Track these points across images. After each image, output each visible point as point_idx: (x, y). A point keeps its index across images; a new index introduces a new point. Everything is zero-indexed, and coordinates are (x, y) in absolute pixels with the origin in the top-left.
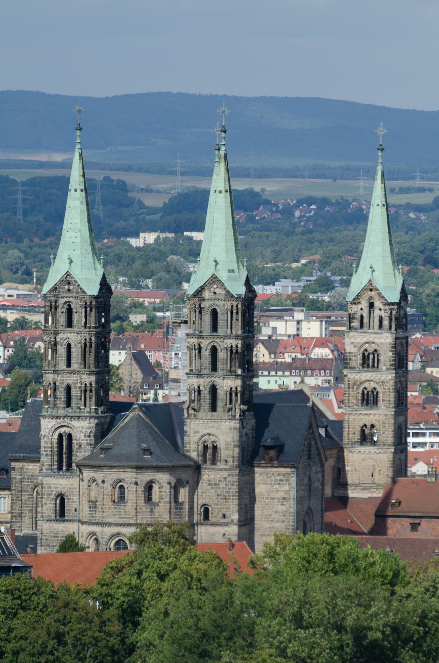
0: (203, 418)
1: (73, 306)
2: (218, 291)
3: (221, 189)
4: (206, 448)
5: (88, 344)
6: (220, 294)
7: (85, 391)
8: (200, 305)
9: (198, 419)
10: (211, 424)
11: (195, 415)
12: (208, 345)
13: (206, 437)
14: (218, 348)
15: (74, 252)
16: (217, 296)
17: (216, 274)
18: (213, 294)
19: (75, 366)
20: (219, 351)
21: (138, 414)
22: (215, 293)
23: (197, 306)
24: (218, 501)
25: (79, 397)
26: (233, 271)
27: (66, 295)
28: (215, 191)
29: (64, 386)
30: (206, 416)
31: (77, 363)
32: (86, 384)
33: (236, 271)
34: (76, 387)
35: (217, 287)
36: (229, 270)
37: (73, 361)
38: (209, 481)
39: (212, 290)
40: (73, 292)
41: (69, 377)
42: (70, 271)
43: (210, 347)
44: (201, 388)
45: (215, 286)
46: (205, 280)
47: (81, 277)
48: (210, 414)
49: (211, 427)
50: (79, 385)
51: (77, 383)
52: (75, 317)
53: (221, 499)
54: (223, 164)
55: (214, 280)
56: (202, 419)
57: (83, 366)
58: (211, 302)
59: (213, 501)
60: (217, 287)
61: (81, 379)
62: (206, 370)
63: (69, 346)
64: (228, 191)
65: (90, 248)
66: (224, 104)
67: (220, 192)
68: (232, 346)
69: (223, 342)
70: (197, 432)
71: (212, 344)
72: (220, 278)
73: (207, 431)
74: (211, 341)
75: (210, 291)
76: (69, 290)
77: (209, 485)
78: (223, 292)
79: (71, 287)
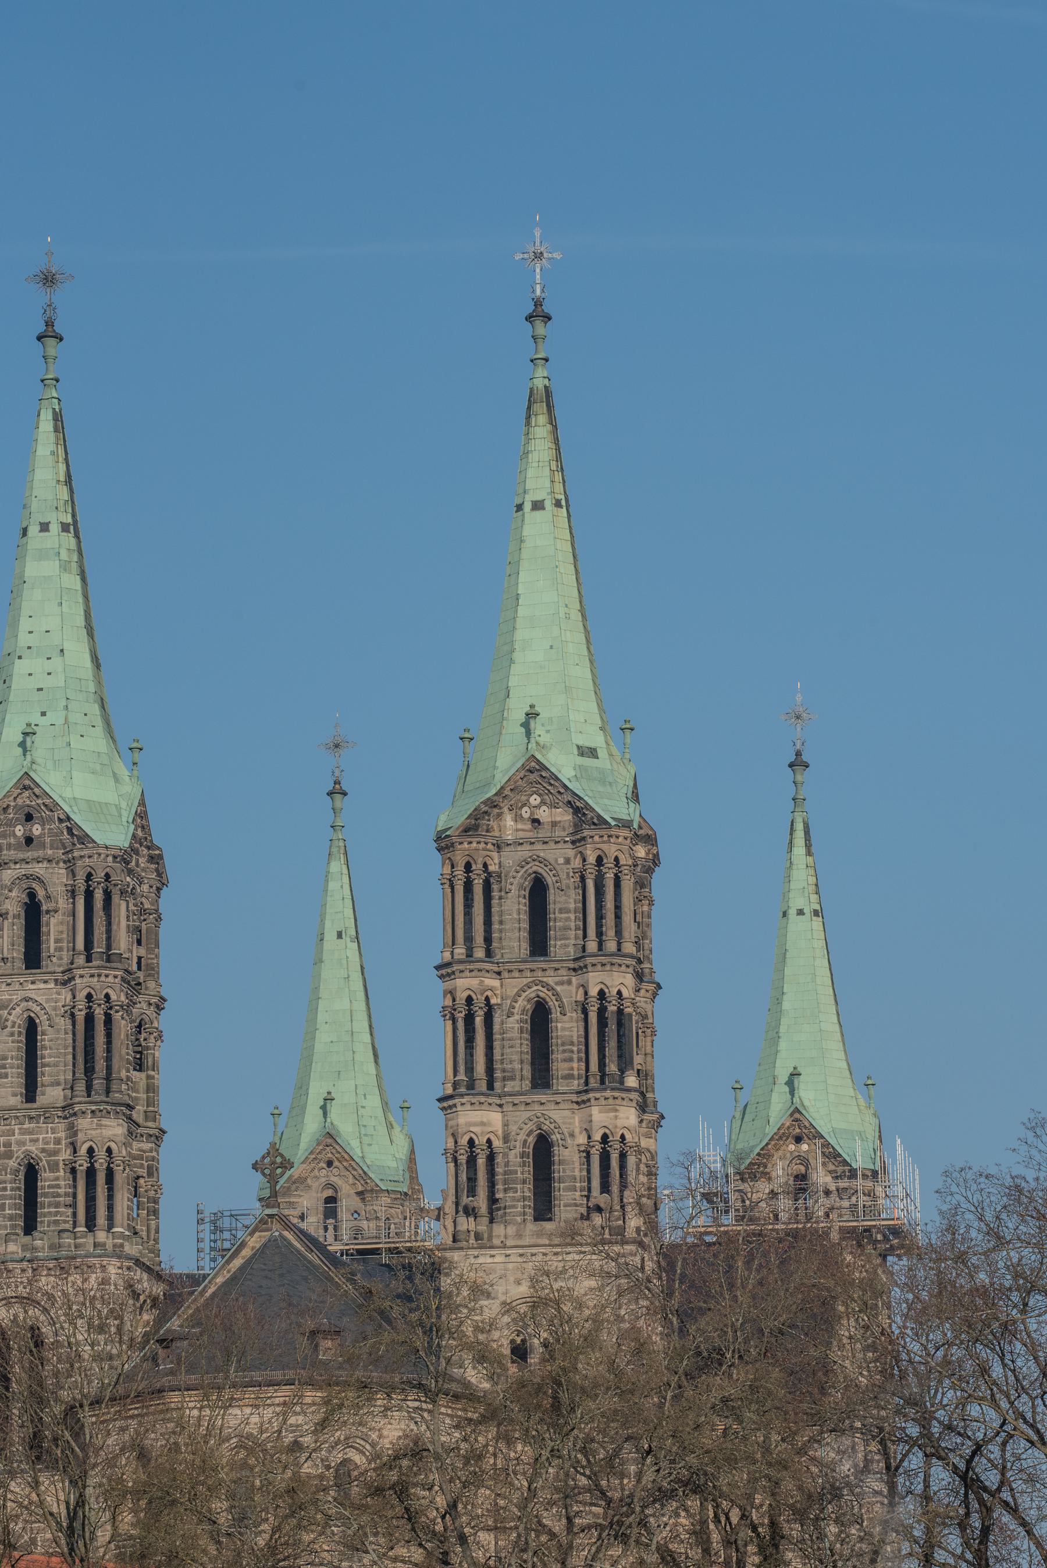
0: (509, 1243)
1: (41, 894)
2: (544, 814)
3: (538, 497)
5: (99, 1012)
6: (554, 824)
7: (91, 1173)
8: (485, 865)
9: (492, 1247)
11: (478, 1237)
14: (552, 1004)
15: (42, 721)
16: (543, 833)
17: (539, 757)
18: (529, 826)
19: (51, 1095)
20: (555, 1014)
21: (281, 1235)
22: (536, 822)
23: (477, 867)
25: (69, 1200)
26: (592, 753)
27: (21, 855)
28: (519, 508)
29: (12, 1163)
30: (519, 1236)
31: (58, 1084)
32: (91, 1151)
33: (602, 753)
34: (54, 1167)
35: (543, 803)
36: (578, 747)
37: (45, 1076)
39: (526, 812)
40: (43, 846)
41: (31, 1133)
42: (32, 774)
43: (521, 1003)
44: (497, 1143)
46: (500, 779)
47: (68, 793)
48: (531, 1227)
50: (65, 1155)
51: (56, 1153)
52: (54, 927)
54: (542, 419)
55: (533, 777)
56: (504, 1246)
57: (81, 1086)
58: (524, 852)
60: (543, 803)
61: (75, 1134)
62: (512, 1083)
63: (31, 1029)
64: (563, 503)
65: (96, 709)
66: (538, 233)
67: (538, 506)
68: (602, 994)
69: (569, 982)
71: (531, 993)
72: (553, 770)
74: (525, 981)
75: (518, 818)
76: (29, 841)
78: (564, 816)
79: (37, 830)
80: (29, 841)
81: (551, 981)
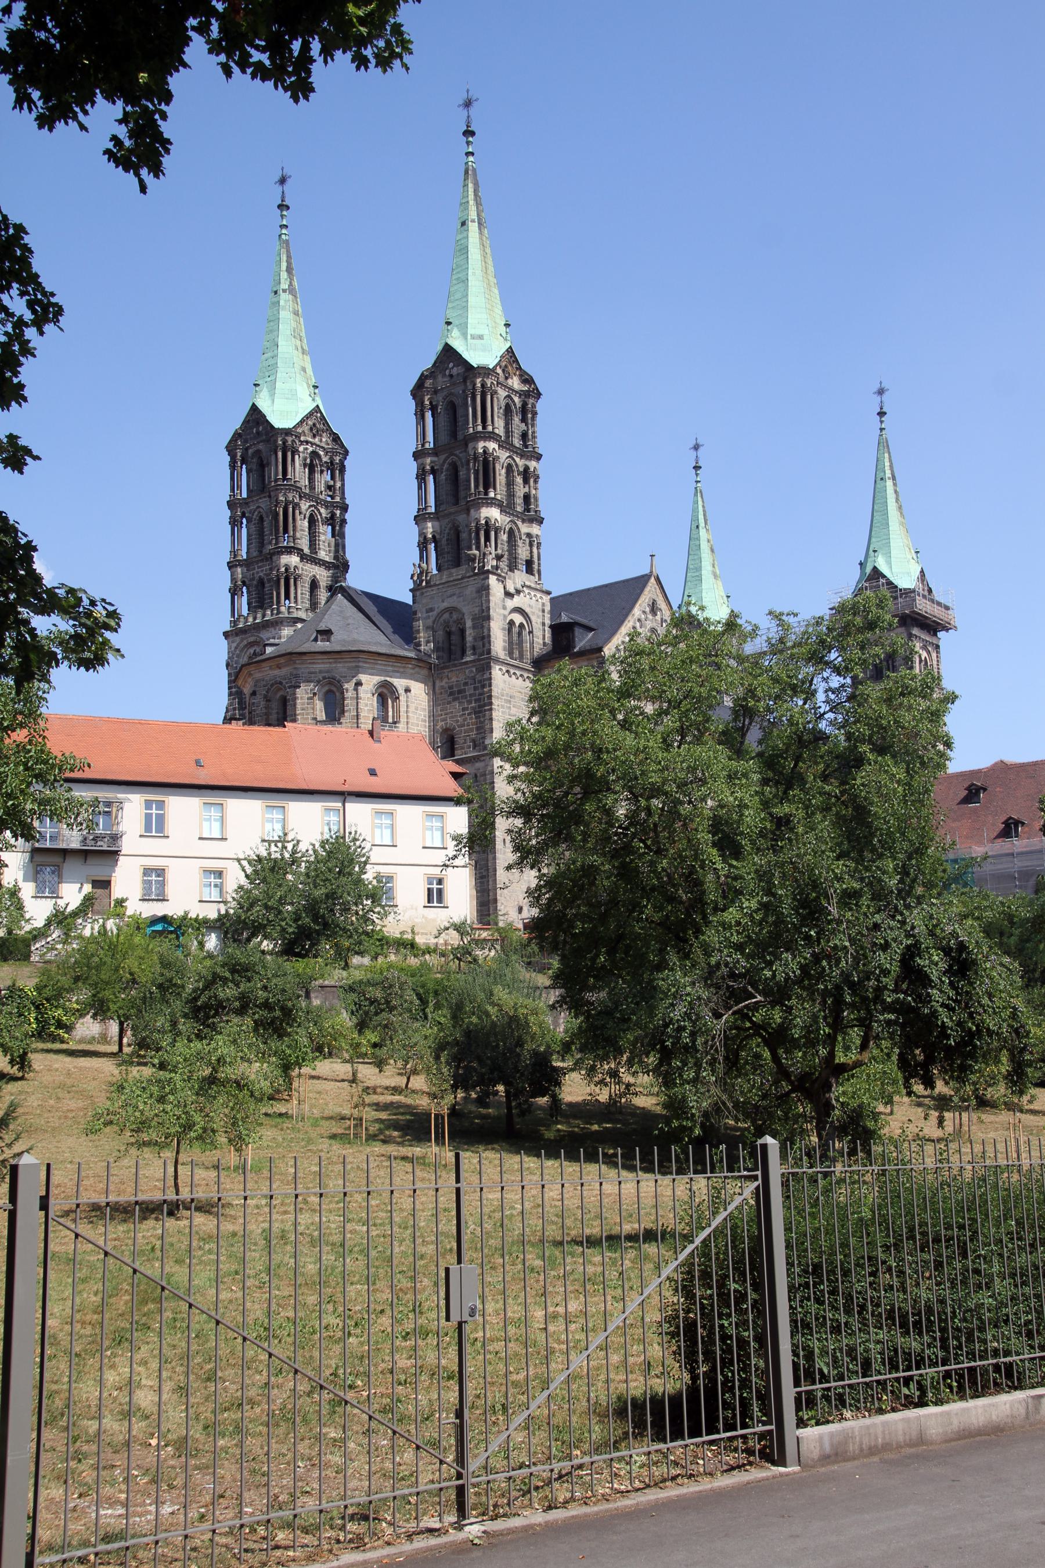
2: (455, 371)
4: (449, 634)
10: (450, 592)
12: (444, 462)
13: (446, 616)
22: (451, 376)
24: (464, 720)
38: (451, 688)
39: (447, 372)
43: (446, 466)
44: (438, 537)
45: (451, 365)
49: (451, 596)
53: (469, 714)
59: (457, 721)
70: (431, 610)
73: (445, 605)
75: (444, 375)
77: (451, 694)
80: (258, 433)
81: (457, 452)
